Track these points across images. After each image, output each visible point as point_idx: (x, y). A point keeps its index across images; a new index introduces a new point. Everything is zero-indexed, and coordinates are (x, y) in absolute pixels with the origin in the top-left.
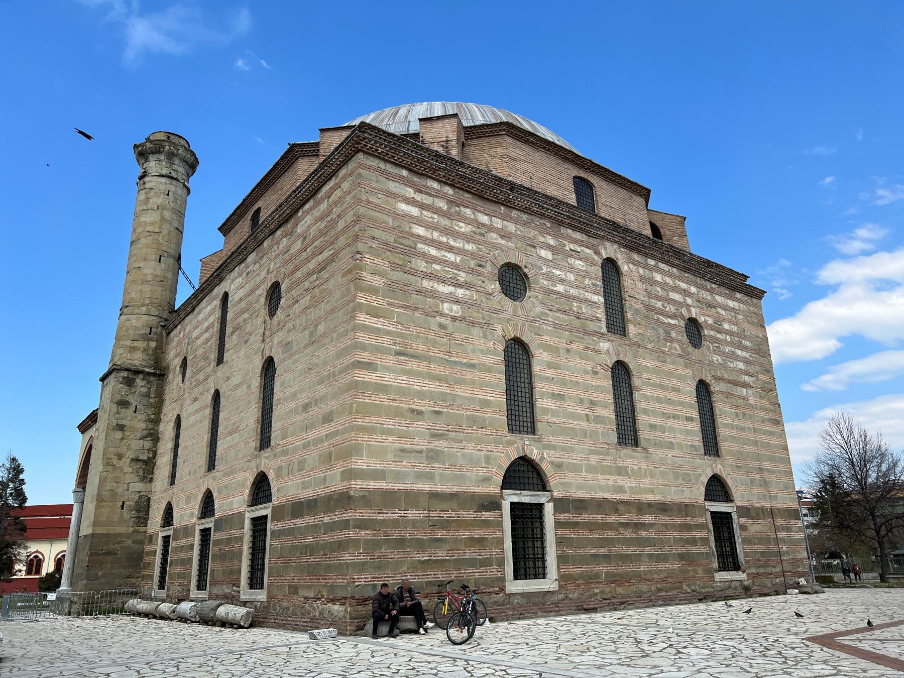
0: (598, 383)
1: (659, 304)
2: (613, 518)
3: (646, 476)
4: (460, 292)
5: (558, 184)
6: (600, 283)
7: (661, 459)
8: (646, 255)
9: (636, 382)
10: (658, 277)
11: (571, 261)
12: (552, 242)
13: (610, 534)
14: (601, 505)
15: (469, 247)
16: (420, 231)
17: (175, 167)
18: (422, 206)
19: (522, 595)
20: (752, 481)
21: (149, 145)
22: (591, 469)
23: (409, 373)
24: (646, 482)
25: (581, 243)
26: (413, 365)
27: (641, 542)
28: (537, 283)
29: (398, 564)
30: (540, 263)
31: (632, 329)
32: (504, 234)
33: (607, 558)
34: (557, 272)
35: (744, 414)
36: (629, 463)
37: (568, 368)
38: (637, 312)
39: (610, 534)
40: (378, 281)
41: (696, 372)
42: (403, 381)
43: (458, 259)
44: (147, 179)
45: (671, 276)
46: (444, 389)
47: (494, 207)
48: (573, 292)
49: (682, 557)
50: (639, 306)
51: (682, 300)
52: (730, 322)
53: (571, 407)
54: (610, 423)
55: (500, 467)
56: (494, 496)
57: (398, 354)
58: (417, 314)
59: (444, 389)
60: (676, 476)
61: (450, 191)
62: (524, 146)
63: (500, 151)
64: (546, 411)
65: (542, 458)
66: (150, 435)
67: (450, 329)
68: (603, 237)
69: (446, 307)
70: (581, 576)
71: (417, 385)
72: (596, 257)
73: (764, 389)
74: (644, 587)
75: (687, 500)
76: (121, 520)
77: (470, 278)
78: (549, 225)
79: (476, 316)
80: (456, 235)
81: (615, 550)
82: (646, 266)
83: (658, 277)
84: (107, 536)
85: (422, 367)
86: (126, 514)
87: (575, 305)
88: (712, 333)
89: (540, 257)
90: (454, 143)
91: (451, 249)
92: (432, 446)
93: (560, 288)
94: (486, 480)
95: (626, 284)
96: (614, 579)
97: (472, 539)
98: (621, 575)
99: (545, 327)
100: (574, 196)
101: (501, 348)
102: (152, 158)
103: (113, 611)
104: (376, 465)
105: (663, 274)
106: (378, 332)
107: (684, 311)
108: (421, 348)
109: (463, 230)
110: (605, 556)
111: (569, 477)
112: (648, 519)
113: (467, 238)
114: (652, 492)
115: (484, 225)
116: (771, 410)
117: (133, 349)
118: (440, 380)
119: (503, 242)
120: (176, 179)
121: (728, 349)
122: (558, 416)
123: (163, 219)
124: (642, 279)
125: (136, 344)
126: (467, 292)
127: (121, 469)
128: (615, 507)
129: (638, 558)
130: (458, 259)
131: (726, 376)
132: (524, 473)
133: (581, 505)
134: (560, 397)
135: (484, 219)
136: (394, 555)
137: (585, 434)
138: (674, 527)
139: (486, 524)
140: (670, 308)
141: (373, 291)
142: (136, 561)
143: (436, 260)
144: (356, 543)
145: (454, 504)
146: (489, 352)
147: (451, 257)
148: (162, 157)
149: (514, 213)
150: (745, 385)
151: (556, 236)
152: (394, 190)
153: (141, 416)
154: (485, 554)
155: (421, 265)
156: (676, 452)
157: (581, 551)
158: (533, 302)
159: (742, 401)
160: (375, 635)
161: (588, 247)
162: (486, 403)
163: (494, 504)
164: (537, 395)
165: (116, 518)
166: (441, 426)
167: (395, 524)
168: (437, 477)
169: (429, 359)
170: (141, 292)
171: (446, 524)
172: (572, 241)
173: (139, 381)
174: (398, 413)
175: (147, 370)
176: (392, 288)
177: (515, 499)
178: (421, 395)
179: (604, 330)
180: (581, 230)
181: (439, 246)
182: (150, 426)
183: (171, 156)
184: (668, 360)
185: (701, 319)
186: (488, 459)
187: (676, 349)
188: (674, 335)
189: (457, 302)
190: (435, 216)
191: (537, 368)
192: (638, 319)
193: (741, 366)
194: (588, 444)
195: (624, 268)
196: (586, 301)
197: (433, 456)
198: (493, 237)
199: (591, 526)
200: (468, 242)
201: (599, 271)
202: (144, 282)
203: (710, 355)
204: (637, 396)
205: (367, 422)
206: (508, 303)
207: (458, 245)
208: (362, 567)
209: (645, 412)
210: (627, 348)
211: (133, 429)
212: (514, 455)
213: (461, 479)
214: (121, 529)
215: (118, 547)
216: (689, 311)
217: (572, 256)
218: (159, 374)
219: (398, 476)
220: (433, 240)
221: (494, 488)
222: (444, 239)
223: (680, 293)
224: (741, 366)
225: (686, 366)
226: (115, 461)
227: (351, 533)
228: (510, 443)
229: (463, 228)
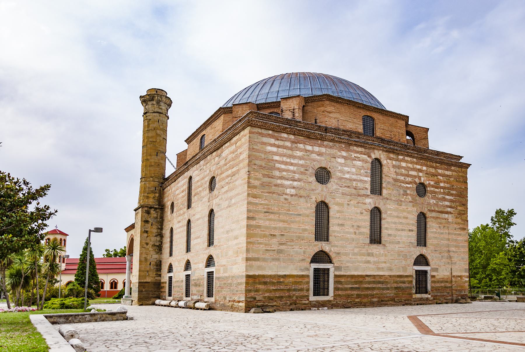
0: (363, 218)
1: (402, 178)
4: (295, 184)
6: (369, 171)
8: (398, 154)
9: (383, 216)
10: (404, 164)
11: (354, 162)
15: (301, 162)
16: (276, 158)
18: (278, 147)
20: (442, 257)
30: (337, 165)
31: (384, 192)
32: (319, 154)
34: (346, 169)
35: (444, 226)
38: (389, 183)
41: (419, 209)
45: (411, 163)
46: (286, 225)
47: (315, 141)
48: (354, 177)
50: (391, 180)
51: (416, 174)
52: (445, 182)
58: (274, 195)
59: (286, 225)
61: (292, 137)
62: (335, 104)
64: (334, 231)
67: (289, 201)
69: (288, 191)
73: (459, 214)
79: (302, 193)
80: (294, 157)
82: (397, 160)
85: (276, 217)
87: (354, 183)
88: (432, 189)
89: (338, 162)
90: (297, 110)
91: (292, 164)
92: (279, 248)
93: (347, 176)
99: (337, 195)
101: (314, 206)
105: (406, 163)
107: (417, 180)
108: (276, 209)
109: (298, 155)
113: (300, 158)
115: (309, 151)
116: (462, 224)
118: (284, 222)
119: (318, 157)
121: (440, 196)
122: (340, 233)
124: (394, 166)
126: (299, 183)
130: (295, 168)
131: (437, 209)
132: (321, 257)
134: (342, 225)
135: (309, 148)
140: (409, 179)
146: (308, 208)
149: (326, 143)
150: (447, 213)
155: (277, 173)
158: (332, 185)
159: (444, 220)
161: (365, 154)
162: (305, 230)
164: (330, 225)
166: (284, 240)
169: (279, 214)
175: (155, 206)
177: (316, 267)
178: (275, 228)
179: (369, 193)
180: (361, 146)
181: (286, 163)
184: (403, 204)
185: (427, 183)
187: (409, 199)
188: (408, 192)
189: (294, 188)
190: (285, 150)
193: (447, 203)
195: (384, 162)
196: (361, 181)
198: (314, 156)
201: (369, 165)
203: (430, 200)
204: (383, 222)
207: (295, 162)
210: (381, 201)
212: (316, 250)
216: (420, 179)
217: (355, 160)
218: (161, 207)
222: (288, 160)
223: (416, 171)
224: (447, 203)
225: (413, 206)
228: (315, 246)
229: (299, 154)
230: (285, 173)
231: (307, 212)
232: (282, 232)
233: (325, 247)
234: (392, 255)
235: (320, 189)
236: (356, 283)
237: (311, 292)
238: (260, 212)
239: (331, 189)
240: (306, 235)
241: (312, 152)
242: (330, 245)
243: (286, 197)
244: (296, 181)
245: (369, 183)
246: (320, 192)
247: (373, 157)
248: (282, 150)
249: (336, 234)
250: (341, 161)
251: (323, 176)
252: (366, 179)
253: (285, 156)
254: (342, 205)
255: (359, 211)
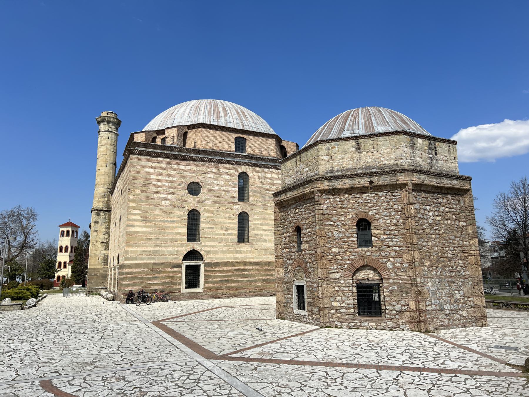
1: (268, 187)
2: (232, 268)
3: (250, 253)
4: (169, 196)
5: (227, 143)
7: (259, 246)
8: (264, 168)
9: (250, 219)
10: (269, 175)
12: (214, 170)
13: (229, 274)
14: (226, 264)
15: (175, 179)
16: (154, 177)
17: (110, 126)
18: (155, 168)
19: (188, 293)
21: (100, 119)
22: (223, 252)
23: (148, 226)
24: (250, 255)
25: (229, 168)
26: (149, 224)
27: (243, 276)
28: (205, 187)
29: (140, 284)
30: (207, 180)
31: (251, 199)
32: (190, 171)
33: (227, 282)
34: (215, 182)
36: (242, 249)
37: (217, 217)
38: (255, 191)
39: (229, 274)
40: (136, 198)
42: (144, 229)
43: (170, 184)
44: (100, 133)
46: (161, 230)
48: (223, 188)
49: (264, 281)
53: (216, 231)
54: (235, 235)
55: (183, 254)
56: (179, 263)
57: (143, 221)
59: (161, 230)
60: (266, 252)
61: (168, 160)
63: (199, 134)
64: (204, 234)
65: (201, 250)
66: (107, 233)
67: (164, 210)
68: (240, 165)
69: (163, 203)
70: (214, 287)
71: (149, 230)
72: (236, 173)
74: (243, 291)
75: (270, 261)
76: (99, 264)
77: (174, 190)
78: (213, 164)
80: (169, 176)
81: (230, 279)
83: (269, 175)
84: (95, 269)
85: (152, 224)
86: (100, 261)
89: (208, 177)
90: (175, 137)
93: (216, 188)
94: (176, 258)
95: (250, 181)
96: (228, 288)
97: (169, 277)
98: (233, 287)
100: (234, 146)
102: (102, 124)
103: (98, 294)
104: (133, 256)
106: (135, 214)
108: (152, 218)
110: (226, 281)
111: (213, 255)
112: (249, 268)
113: (174, 176)
114: (253, 258)
115: (182, 170)
117: (99, 202)
119: (190, 174)
120: (112, 132)
122: (210, 235)
123: (107, 149)
124: (259, 178)
125: (100, 200)
126: (173, 196)
127: (97, 246)
128: (233, 264)
129: (242, 281)
130: (170, 184)
133: (217, 264)
135: (182, 167)
136: (140, 282)
137: (222, 240)
138: (262, 270)
139: (175, 272)
141: (134, 201)
142: (105, 277)
143: (159, 186)
144: (126, 279)
145: (163, 266)
146: (181, 216)
147: (167, 184)
148: (105, 123)
149: (196, 163)
151: (216, 168)
152: (144, 165)
153: (103, 227)
154: (174, 281)
155: (154, 189)
156: (268, 243)
157: (215, 279)
158: (203, 195)
160: (127, 303)
161: (232, 170)
162: (178, 233)
163: (179, 266)
165: (97, 263)
166: (159, 242)
167: (140, 273)
168: (156, 259)
169: (155, 221)
170: (101, 179)
171: (159, 272)
172: (224, 168)
173: (102, 214)
174: (142, 240)
176: (141, 200)
177: (188, 264)
178: (151, 233)
180: (229, 164)
181: (162, 181)
182: (107, 230)
183: (108, 122)
186: (177, 252)
191: (202, 219)
192: (255, 194)
194: (223, 243)
195: (250, 175)
196: (229, 191)
197: (155, 252)
198: (186, 173)
199: (220, 271)
200: (174, 177)
202: (102, 175)
205: (131, 243)
206: (191, 197)
207: (170, 179)
208: (128, 285)
209: (253, 229)
211: (101, 232)
212: (189, 249)
213: (166, 258)
214: (99, 267)
215: (98, 273)
219: (141, 259)
220: (159, 179)
221: (179, 261)
222: (164, 178)
226: (95, 243)
227: (125, 276)
228: (187, 246)
229: (173, 172)
230: (160, 189)
231: (180, 219)
232: (157, 235)
233: (195, 246)
234: (259, 252)
235: (192, 200)
236: (225, 276)
237: (183, 285)
238: (139, 220)
239: (202, 199)
240: (179, 237)
241: (185, 170)
242: (201, 245)
243: (161, 207)
244: (170, 194)
245: (237, 193)
246: (193, 202)
247: (240, 171)
248: (158, 170)
249: (206, 236)
250: (212, 176)
251: (194, 189)
252: (233, 189)
253: (160, 175)
254: (212, 211)
255: (227, 216)
